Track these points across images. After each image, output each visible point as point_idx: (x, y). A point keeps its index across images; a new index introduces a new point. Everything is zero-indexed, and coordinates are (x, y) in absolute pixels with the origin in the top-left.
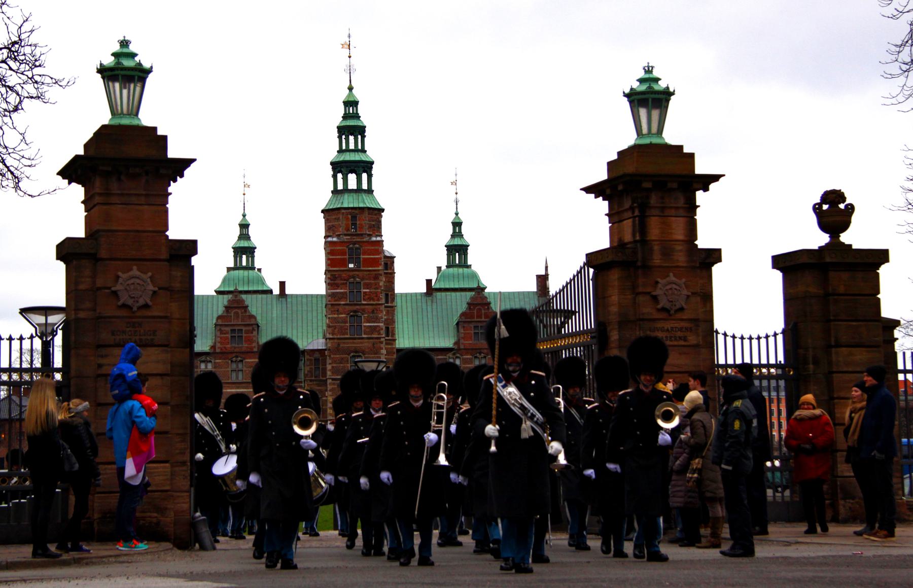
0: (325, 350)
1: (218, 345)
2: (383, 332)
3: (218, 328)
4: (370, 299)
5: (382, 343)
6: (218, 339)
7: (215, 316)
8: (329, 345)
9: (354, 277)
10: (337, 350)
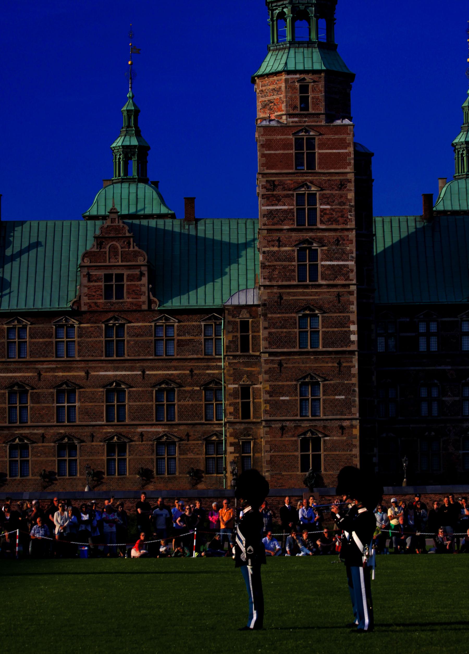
0: (258, 306)
1: (85, 300)
2: (353, 275)
3: (85, 271)
4: (332, 220)
5: (351, 293)
6: (86, 290)
7: (81, 251)
8: (265, 298)
9: (304, 184)
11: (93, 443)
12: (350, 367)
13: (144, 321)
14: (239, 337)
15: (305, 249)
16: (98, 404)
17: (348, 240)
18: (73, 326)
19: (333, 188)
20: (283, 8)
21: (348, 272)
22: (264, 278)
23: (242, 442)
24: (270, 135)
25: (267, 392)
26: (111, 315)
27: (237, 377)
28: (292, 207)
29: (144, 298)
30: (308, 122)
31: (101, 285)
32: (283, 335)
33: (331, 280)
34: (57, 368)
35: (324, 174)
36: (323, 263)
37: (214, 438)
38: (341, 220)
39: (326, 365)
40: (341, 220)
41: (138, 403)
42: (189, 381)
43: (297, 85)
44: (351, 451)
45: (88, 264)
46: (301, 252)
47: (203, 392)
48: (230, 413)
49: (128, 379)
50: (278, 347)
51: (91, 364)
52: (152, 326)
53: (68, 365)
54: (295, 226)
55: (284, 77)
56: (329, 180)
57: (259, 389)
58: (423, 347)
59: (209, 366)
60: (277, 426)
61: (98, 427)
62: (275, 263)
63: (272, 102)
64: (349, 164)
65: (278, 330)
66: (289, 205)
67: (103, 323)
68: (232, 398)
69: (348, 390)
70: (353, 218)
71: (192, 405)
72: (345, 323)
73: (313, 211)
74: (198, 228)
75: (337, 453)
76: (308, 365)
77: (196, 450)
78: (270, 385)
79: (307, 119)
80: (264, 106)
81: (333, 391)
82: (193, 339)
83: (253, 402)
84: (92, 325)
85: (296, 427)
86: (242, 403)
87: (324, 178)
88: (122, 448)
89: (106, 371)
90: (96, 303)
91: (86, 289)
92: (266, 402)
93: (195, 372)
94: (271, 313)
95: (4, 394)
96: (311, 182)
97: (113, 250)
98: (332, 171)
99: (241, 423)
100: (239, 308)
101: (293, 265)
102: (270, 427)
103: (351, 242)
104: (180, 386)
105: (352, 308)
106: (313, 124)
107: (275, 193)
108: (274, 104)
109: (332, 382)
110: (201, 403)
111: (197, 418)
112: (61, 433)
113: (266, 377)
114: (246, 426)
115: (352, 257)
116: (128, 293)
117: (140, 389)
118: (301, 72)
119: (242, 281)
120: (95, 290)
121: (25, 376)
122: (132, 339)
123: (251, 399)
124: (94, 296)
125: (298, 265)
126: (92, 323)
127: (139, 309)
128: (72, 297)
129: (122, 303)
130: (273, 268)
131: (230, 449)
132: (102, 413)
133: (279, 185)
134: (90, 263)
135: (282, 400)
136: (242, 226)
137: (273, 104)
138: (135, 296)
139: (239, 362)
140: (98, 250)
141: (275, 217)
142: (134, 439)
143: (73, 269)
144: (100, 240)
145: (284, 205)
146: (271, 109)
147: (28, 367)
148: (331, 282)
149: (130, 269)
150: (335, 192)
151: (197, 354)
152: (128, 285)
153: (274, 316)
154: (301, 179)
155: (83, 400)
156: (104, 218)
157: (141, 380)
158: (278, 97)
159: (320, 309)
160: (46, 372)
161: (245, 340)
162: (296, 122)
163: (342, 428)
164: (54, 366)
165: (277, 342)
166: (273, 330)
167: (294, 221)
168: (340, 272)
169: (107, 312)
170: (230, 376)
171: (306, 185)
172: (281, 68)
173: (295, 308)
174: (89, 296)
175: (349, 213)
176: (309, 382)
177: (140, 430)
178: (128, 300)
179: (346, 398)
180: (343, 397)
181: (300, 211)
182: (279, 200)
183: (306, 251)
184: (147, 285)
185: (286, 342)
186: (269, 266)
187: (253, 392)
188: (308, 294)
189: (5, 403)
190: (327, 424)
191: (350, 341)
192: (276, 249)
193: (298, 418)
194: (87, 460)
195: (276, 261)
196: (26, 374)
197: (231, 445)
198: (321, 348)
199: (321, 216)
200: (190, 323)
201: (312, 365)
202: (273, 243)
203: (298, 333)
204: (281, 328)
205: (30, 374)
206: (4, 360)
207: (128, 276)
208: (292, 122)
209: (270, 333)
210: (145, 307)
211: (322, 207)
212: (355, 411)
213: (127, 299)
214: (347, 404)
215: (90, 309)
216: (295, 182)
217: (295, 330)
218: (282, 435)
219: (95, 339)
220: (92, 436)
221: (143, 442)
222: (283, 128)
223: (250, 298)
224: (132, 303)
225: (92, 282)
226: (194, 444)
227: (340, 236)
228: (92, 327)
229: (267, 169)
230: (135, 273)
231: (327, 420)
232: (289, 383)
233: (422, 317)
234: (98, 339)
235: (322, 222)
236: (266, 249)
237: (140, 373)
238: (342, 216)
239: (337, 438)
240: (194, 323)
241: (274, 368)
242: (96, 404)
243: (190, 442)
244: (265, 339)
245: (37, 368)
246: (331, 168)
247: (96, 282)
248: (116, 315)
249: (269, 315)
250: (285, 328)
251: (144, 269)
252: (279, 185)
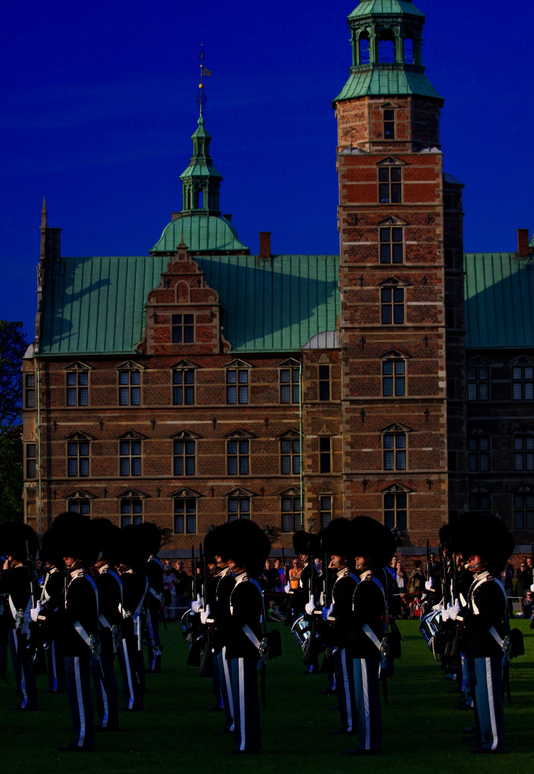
0: (339, 350)
1: (151, 342)
2: (442, 317)
3: (151, 312)
5: (439, 336)
6: (152, 332)
8: (347, 341)
9: (388, 218)
11: (160, 499)
12: (438, 416)
13: (214, 366)
14: (318, 383)
15: (389, 289)
16: (165, 456)
17: (436, 279)
18: (138, 372)
19: (420, 223)
20: (366, 27)
21: (436, 313)
22: (345, 320)
23: (322, 498)
24: (352, 165)
25: (348, 443)
26: (179, 359)
27: (315, 427)
28: (376, 243)
29: (215, 341)
30: (393, 150)
31: (169, 327)
32: (365, 381)
33: (417, 322)
34: (121, 416)
35: (411, 207)
36: (409, 303)
37: (291, 493)
38: (429, 257)
39: (412, 414)
40: (429, 257)
41: (208, 455)
42: (263, 431)
43: (382, 110)
44: (439, 507)
45: (155, 304)
46: (386, 290)
47: (280, 443)
48: (309, 466)
49: (198, 429)
50: (360, 395)
51: (157, 413)
52: (223, 371)
53: (133, 413)
54: (379, 264)
55: (367, 101)
56: (415, 214)
57: (340, 440)
58: (517, 395)
59: (285, 415)
60: (359, 480)
61: (165, 481)
62: (358, 304)
63: (355, 129)
64: (438, 196)
65: (360, 376)
66: (372, 240)
67: (171, 367)
68: (311, 449)
69: (435, 441)
70: (442, 255)
71: (267, 457)
72: (433, 368)
73: (398, 247)
74: (275, 265)
75: (424, 509)
76: (392, 414)
77: (271, 505)
78: (351, 436)
79: (392, 148)
80: (346, 134)
81: (420, 443)
82: (268, 386)
83: (333, 454)
84: (159, 370)
85: (379, 482)
86: (321, 455)
87: (410, 211)
88: (191, 504)
89: (173, 420)
90: (163, 346)
91: (153, 331)
92: (347, 454)
93: (271, 421)
94: (353, 358)
95: (63, 445)
96: (397, 216)
97: (182, 289)
98: (419, 203)
99: (320, 477)
100: (319, 352)
101: (377, 306)
102: (351, 481)
103: (440, 281)
104: (254, 436)
105: (441, 353)
106: (399, 153)
107: (357, 227)
108: (357, 131)
109: (418, 433)
110: (277, 455)
111: (272, 471)
112: (125, 487)
113: (348, 427)
114: (325, 480)
115: (441, 297)
116: (198, 335)
117: (211, 440)
118: (386, 96)
119: (322, 323)
120: (162, 332)
121: (86, 426)
122: (203, 385)
123: (331, 451)
124: (161, 338)
125: (383, 306)
126: (159, 368)
127: (210, 353)
128: (137, 340)
129: (191, 346)
130: (355, 308)
131: (308, 505)
132: (170, 466)
133: (361, 219)
134: (157, 302)
135: (365, 452)
136: (322, 263)
137: (355, 131)
138: (206, 339)
139: (318, 410)
140: (166, 289)
141: (357, 253)
142: (205, 494)
143: (138, 309)
144: (167, 278)
145: (367, 240)
146: (353, 137)
147: (89, 415)
148: (418, 324)
149: (200, 309)
150: (422, 227)
151: (272, 402)
152: (197, 327)
153: (356, 360)
154: (385, 212)
155: (148, 452)
156: (172, 254)
157: (211, 430)
158: (361, 123)
159: (406, 353)
160: (109, 421)
161: (324, 387)
162: (380, 151)
163: (429, 482)
164: (117, 415)
165: (360, 389)
166: (355, 376)
167: (378, 258)
168: (428, 313)
169: (175, 356)
170: (308, 425)
171: (391, 218)
172: (363, 92)
173: (379, 352)
174: (156, 339)
175: (437, 250)
176: (393, 432)
177: (210, 484)
178: (198, 343)
179: (434, 450)
180: (431, 449)
181: (385, 247)
182: (362, 236)
183: (391, 290)
184: (218, 327)
185: (368, 389)
186: (351, 307)
187: (333, 444)
188: (392, 337)
189: (64, 455)
190: (414, 478)
191: (438, 388)
192: (358, 288)
193: (382, 471)
194: (153, 516)
195: (358, 301)
196: (87, 424)
197: (310, 500)
198: (406, 396)
199: (407, 253)
200: (265, 369)
201: (397, 414)
202: (355, 282)
203: (381, 379)
204: (364, 373)
205: (92, 423)
206: (63, 407)
207: (198, 317)
208: (376, 151)
209: (351, 379)
210: (216, 351)
211: (408, 243)
212: (444, 464)
213: (196, 342)
214: (435, 457)
215: (157, 353)
216: (379, 216)
217: (379, 376)
218: (365, 490)
219: (162, 386)
220: (159, 490)
221: (214, 498)
222: (366, 158)
223: (330, 341)
224: (201, 347)
225: (159, 323)
226: (269, 500)
227: (428, 274)
228: (158, 372)
229: (349, 201)
230: (205, 314)
231: (413, 474)
232: (372, 434)
233: (517, 362)
234: (165, 386)
235: (408, 259)
236: (348, 288)
237: (210, 422)
238: (430, 253)
239: (424, 494)
240: (270, 369)
241: (356, 417)
242: (163, 456)
243: (265, 498)
244: (346, 386)
245: (99, 417)
246: (418, 201)
247: (163, 323)
248: (185, 359)
249: (351, 360)
250: (368, 374)
251: (216, 310)
252: (361, 219)
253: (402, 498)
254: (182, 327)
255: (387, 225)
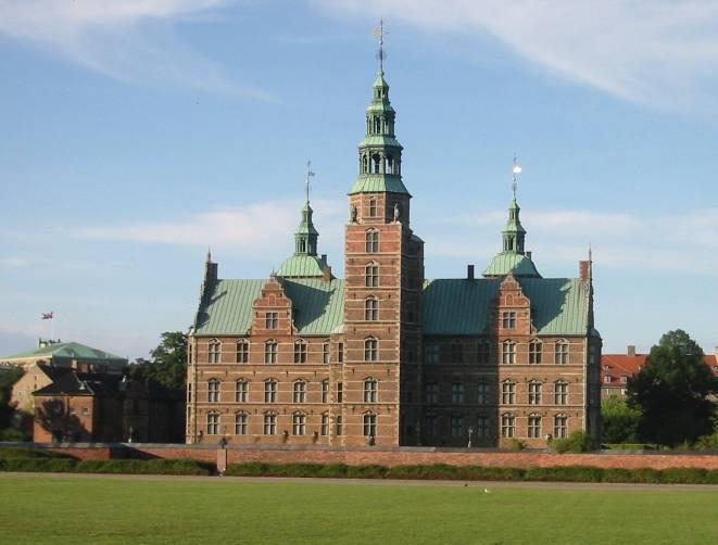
1: (254, 328)
2: (398, 317)
5: (397, 327)
10: (353, 333)
18: (247, 344)
72: (391, 346)
131: (331, 420)
174: (256, 326)
176: (370, 383)
198: (378, 361)
210: (289, 333)
213: (278, 328)
214: (394, 395)
251: (290, 311)
253: (373, 418)
254: (271, 320)
255: (369, 265)
